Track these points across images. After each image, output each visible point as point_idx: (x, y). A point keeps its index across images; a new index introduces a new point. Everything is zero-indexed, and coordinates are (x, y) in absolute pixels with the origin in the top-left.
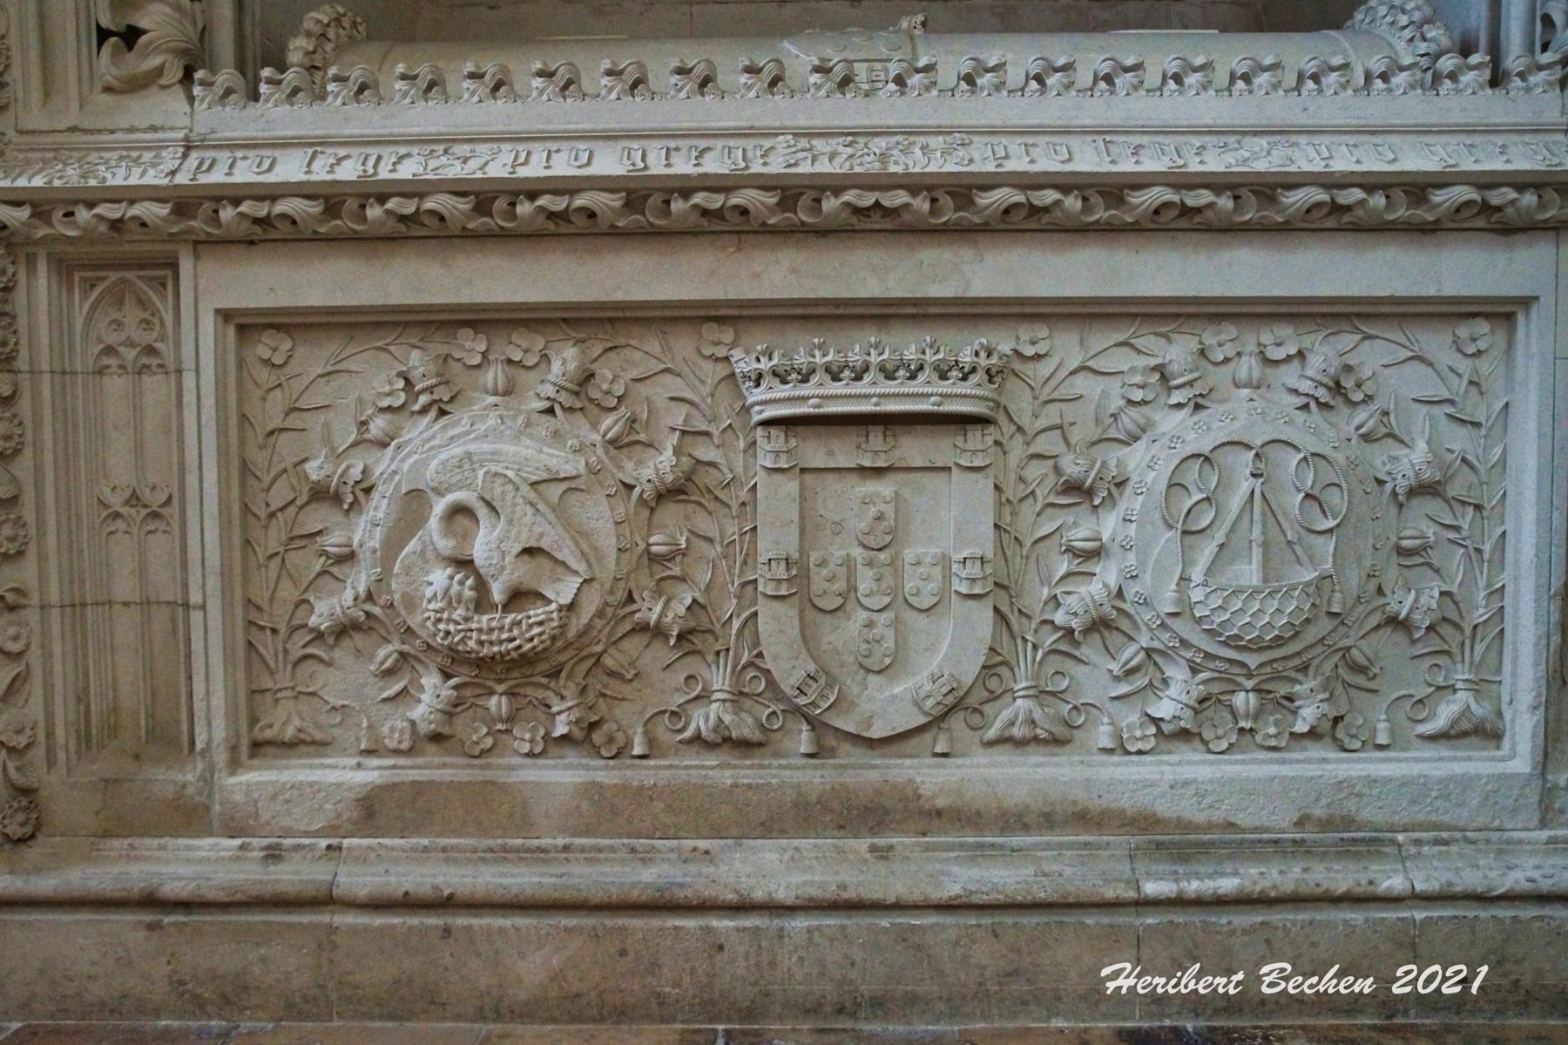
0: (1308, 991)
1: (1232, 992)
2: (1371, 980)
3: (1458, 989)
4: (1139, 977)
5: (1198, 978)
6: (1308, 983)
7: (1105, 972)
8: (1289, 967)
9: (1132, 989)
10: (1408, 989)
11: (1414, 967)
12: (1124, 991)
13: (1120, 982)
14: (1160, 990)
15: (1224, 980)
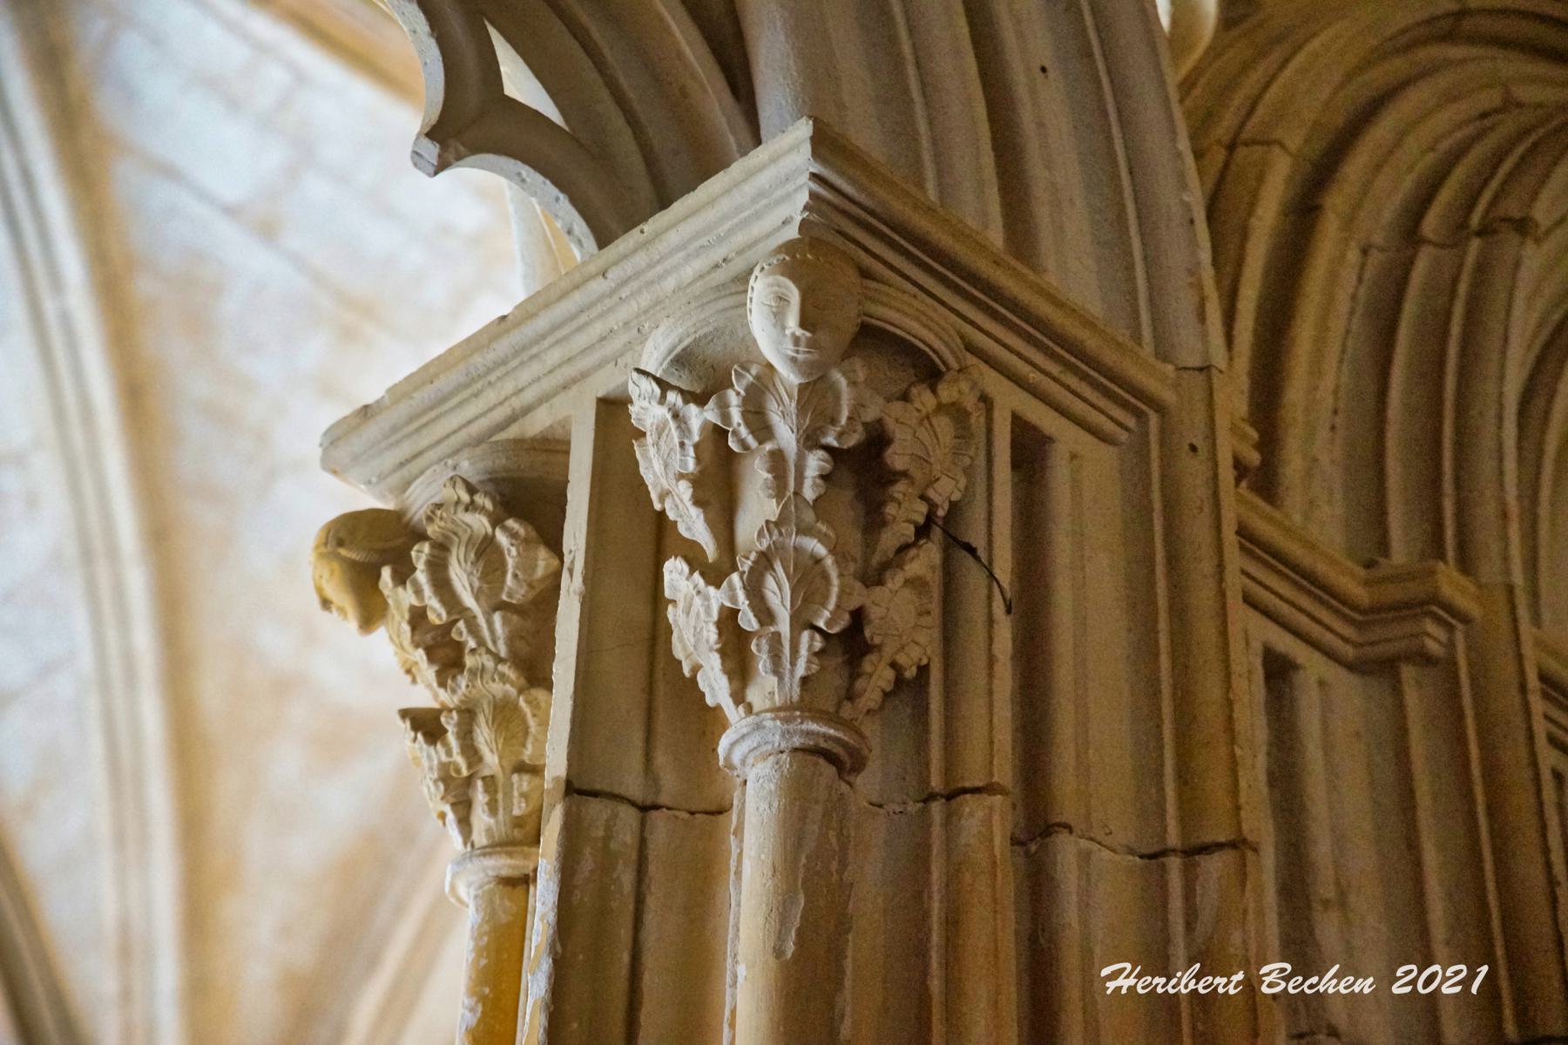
0: (1308, 992)
1: (1232, 992)
2: (1371, 980)
3: (1458, 989)
4: (1139, 977)
5: (1198, 977)
6: (1308, 983)
7: (1105, 972)
8: (1289, 967)
9: (1132, 989)
10: (1408, 989)
11: (1414, 967)
12: (1124, 991)
13: (1120, 981)
14: (1160, 990)
15: (1224, 980)
